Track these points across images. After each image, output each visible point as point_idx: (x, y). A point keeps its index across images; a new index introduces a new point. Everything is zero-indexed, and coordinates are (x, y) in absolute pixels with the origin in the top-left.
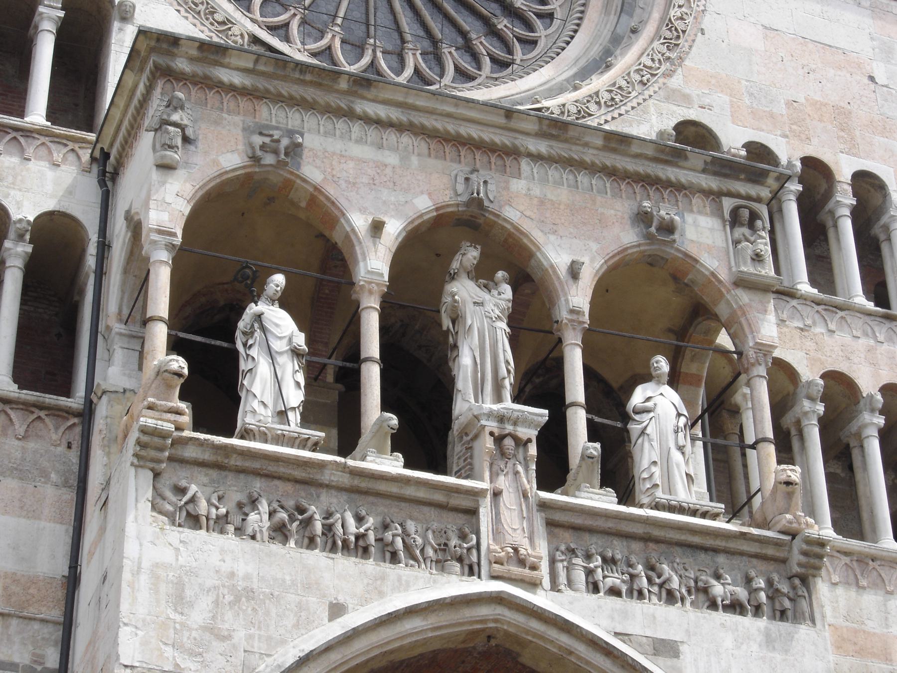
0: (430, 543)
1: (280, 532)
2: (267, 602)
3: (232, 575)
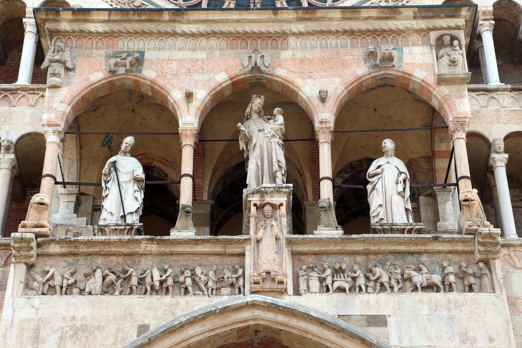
0: (211, 279)
1: (108, 288)
2: (96, 331)
3: (74, 318)
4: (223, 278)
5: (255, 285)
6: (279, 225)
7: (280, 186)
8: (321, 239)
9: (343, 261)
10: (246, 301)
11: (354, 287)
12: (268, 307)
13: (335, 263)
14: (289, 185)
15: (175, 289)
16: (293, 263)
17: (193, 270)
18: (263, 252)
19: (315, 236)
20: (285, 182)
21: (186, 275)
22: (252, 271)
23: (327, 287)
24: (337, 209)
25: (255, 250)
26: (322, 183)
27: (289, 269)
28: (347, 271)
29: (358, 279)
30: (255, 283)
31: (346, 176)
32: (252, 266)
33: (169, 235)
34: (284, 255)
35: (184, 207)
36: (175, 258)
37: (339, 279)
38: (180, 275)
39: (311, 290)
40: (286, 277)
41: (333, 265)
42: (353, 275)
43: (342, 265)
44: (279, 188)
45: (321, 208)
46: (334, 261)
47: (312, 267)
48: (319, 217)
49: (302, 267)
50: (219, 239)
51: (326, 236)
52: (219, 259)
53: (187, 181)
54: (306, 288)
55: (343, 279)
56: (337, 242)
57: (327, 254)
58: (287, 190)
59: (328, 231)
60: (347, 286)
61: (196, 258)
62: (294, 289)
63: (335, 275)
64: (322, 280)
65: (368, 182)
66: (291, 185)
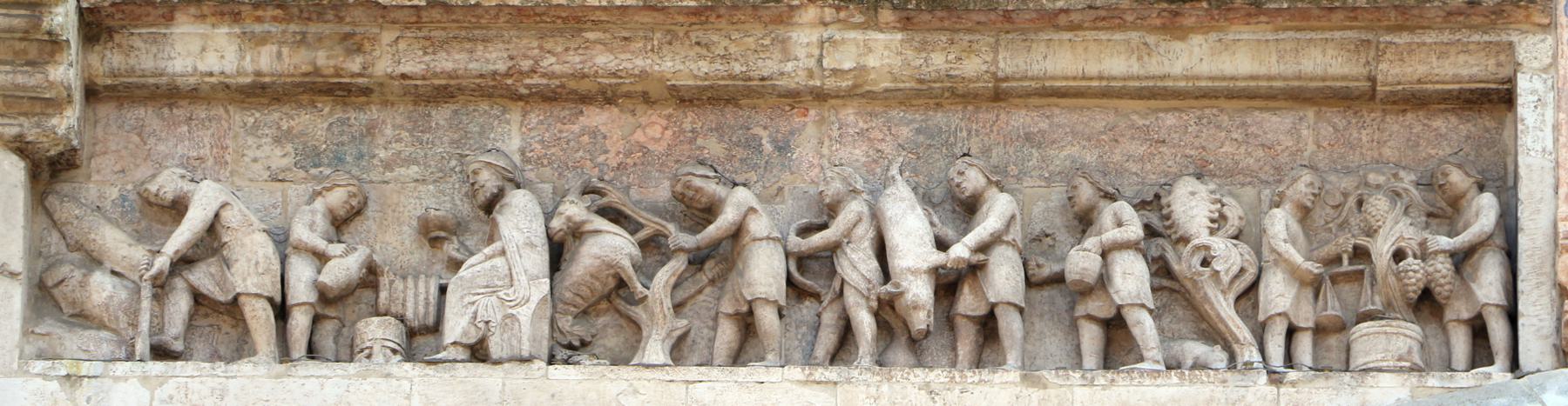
4: (1361, 254)
15: (1039, 325)
21: (1112, 235)
36: (1020, 119)
38: (1063, 236)
52: (1326, 131)
61: (1170, 119)
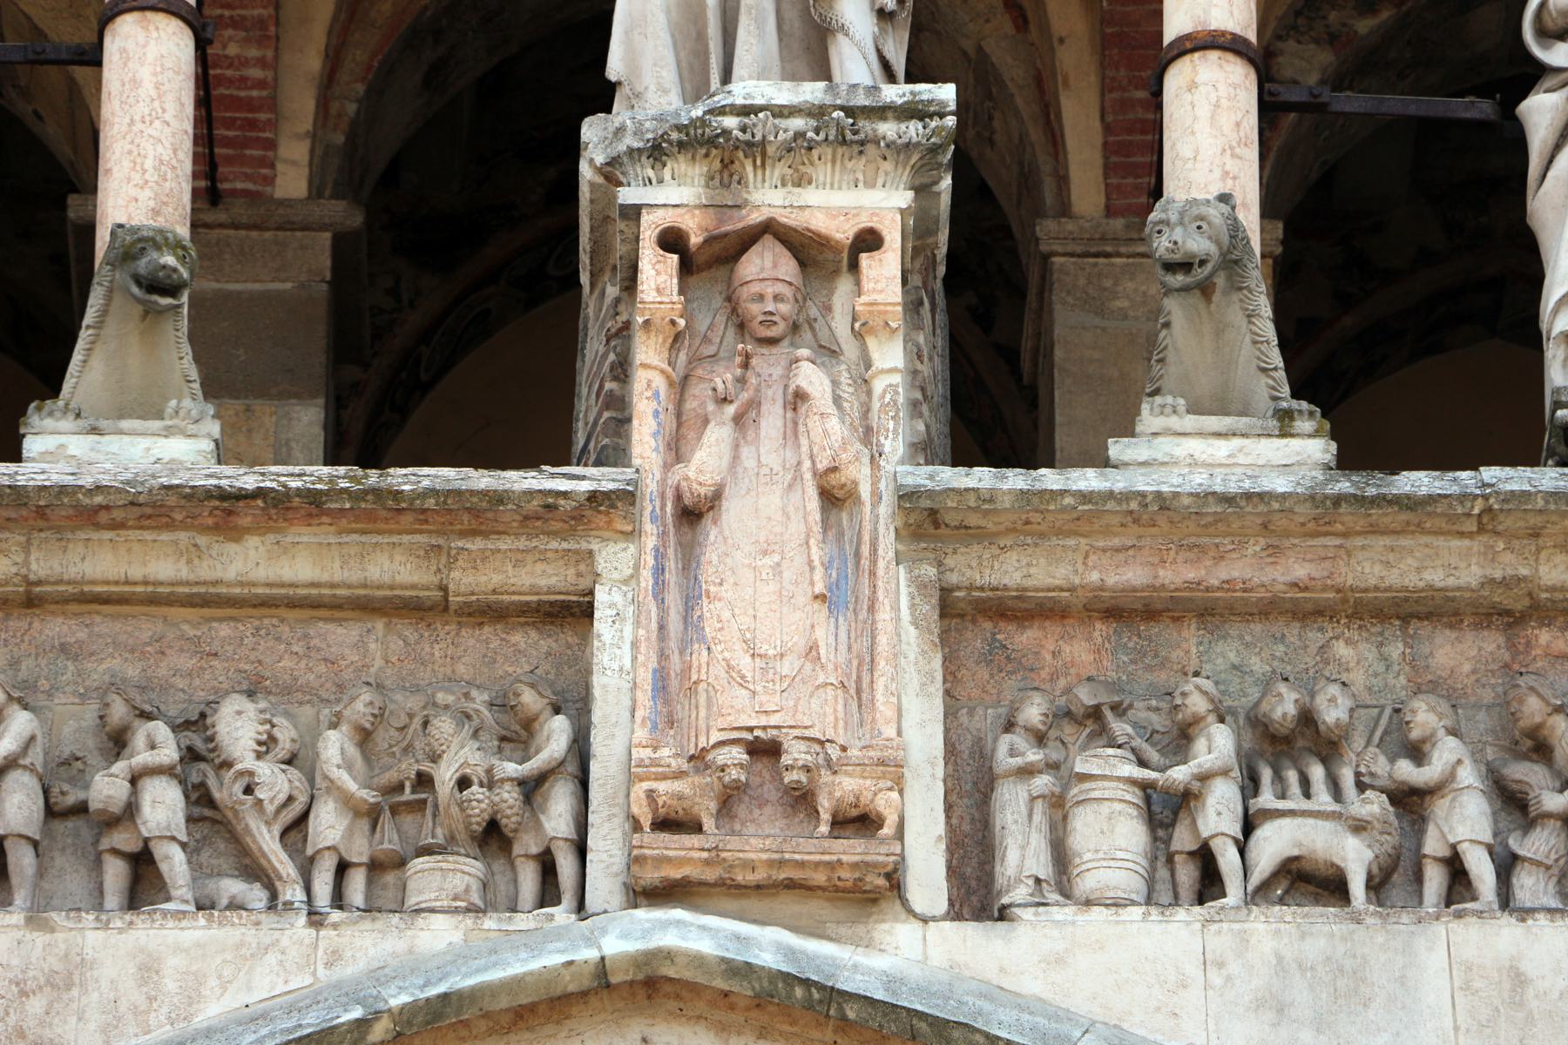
0: (333, 787)
4: (424, 781)
5: (665, 837)
6: (847, 390)
7: (861, 100)
8: (1164, 502)
9: (1324, 670)
10: (591, 954)
11: (1406, 863)
12: (760, 1002)
13: (1267, 685)
14: (925, 90)
15: (59, 860)
16: (951, 675)
17: (196, 726)
18: (726, 592)
19: (1116, 481)
20: (900, 66)
21: (142, 757)
22: (641, 734)
23: (1205, 858)
24: (1288, 276)
25: (671, 577)
26: (1176, 79)
27: (920, 731)
28: (1358, 742)
29: (1439, 808)
30: (667, 824)
31: (1364, 26)
32: (644, 698)
33: (15, 456)
34: (884, 615)
35: (133, 246)
36: (55, 628)
37: (1295, 802)
38: (94, 759)
39: (1087, 883)
40: (899, 785)
41: (1254, 693)
42: (1406, 770)
43: (1321, 702)
44: (849, 111)
45: (1170, 267)
46: (1257, 665)
47: (1095, 713)
48: (1152, 341)
49: (1014, 710)
50: (397, 495)
51: (1198, 480)
52: (396, 644)
53: (152, 51)
54: (1040, 865)
55: (1323, 798)
56: (1280, 522)
57: (1209, 611)
58: (913, 129)
59: (1216, 441)
60: (1355, 858)
61: (225, 630)
62: (952, 871)
63: (1266, 774)
64: (1165, 810)
65: (1532, 74)
66: (947, 93)
